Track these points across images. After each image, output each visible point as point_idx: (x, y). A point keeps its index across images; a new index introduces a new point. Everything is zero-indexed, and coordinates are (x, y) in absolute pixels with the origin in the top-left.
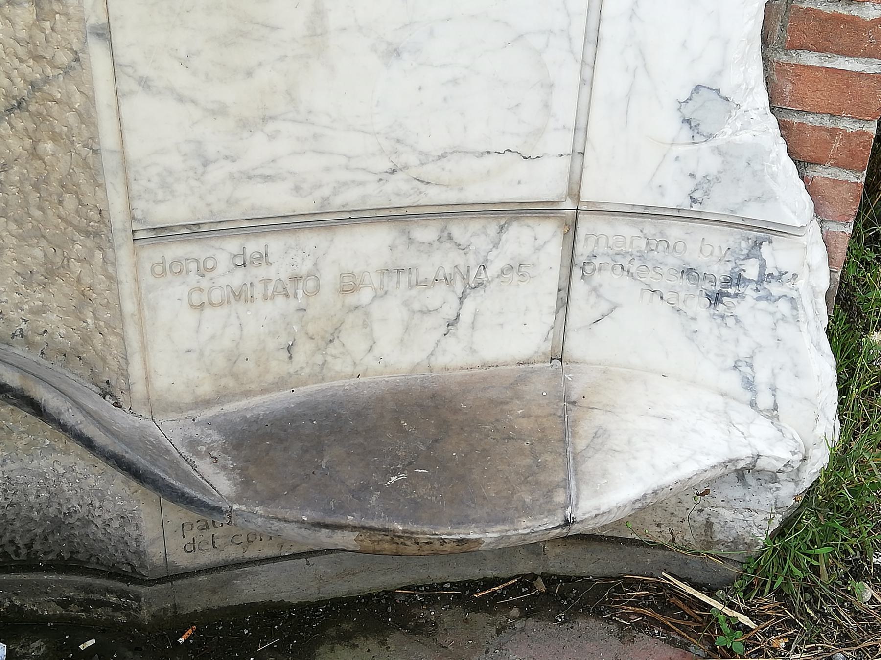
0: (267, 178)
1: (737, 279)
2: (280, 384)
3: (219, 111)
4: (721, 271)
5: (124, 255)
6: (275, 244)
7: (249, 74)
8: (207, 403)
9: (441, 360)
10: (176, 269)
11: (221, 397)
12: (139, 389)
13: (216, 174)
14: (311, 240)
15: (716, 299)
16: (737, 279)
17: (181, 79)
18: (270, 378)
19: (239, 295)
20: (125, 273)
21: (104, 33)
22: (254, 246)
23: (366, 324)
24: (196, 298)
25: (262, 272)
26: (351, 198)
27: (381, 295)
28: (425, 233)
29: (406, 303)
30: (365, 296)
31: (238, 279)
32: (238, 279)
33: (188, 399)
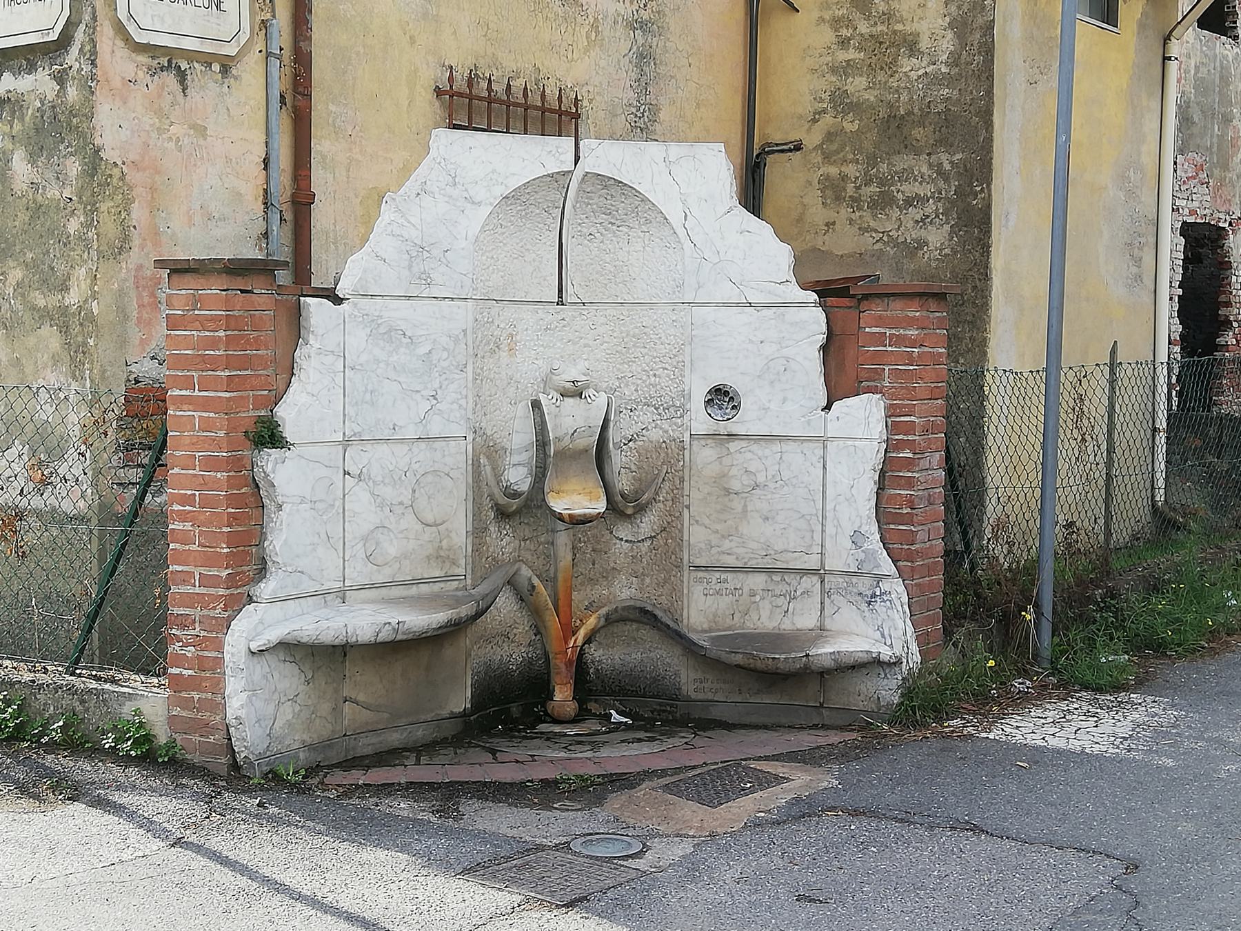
0: (728, 554)
1: (874, 595)
2: (729, 629)
4: (869, 593)
5: (686, 573)
6: (730, 576)
7: (725, 522)
8: (706, 632)
9: (782, 627)
10: (700, 581)
11: (710, 631)
12: (685, 621)
13: (714, 551)
14: (741, 576)
15: (869, 603)
16: (874, 595)
17: (707, 522)
18: (726, 626)
21: (688, 507)
23: (758, 609)
25: (726, 585)
26: (753, 563)
27: (762, 599)
28: (777, 578)
29: (771, 603)
30: (758, 598)
31: (718, 587)
32: (718, 587)
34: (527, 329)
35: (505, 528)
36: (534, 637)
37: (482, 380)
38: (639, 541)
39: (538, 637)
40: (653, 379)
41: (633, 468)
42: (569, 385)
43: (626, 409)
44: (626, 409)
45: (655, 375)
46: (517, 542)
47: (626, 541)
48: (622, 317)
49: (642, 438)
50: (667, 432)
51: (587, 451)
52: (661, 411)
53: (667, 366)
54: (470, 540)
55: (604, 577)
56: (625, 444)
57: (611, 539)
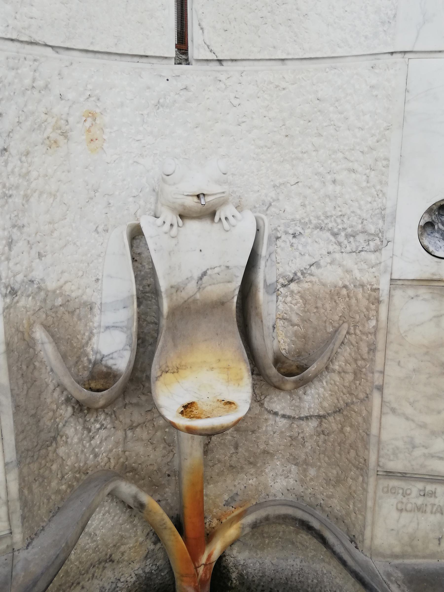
2: (433, 556)
3: (423, 426)
5: (372, 480)
8: (396, 557)
10: (393, 491)
11: (403, 555)
12: (367, 542)
13: (418, 452)
17: (409, 410)
19: (420, 509)
20: (371, 489)
21: (380, 389)
22: (430, 488)
24: (400, 506)
25: (432, 500)
31: (420, 501)
32: (420, 501)
33: (388, 552)
34: (122, 105)
35: (96, 421)
36: (152, 547)
37: (27, 198)
38: (301, 419)
39: (159, 546)
40: (330, 188)
41: (295, 319)
42: (191, 202)
43: (286, 233)
44: (286, 233)
45: (334, 182)
46: (120, 434)
47: (284, 416)
48: (283, 85)
49: (309, 278)
50: (349, 271)
51: (223, 304)
52: (342, 238)
53: (356, 166)
54: (13, 476)
55: (251, 463)
56: (284, 286)
57: (260, 414)
